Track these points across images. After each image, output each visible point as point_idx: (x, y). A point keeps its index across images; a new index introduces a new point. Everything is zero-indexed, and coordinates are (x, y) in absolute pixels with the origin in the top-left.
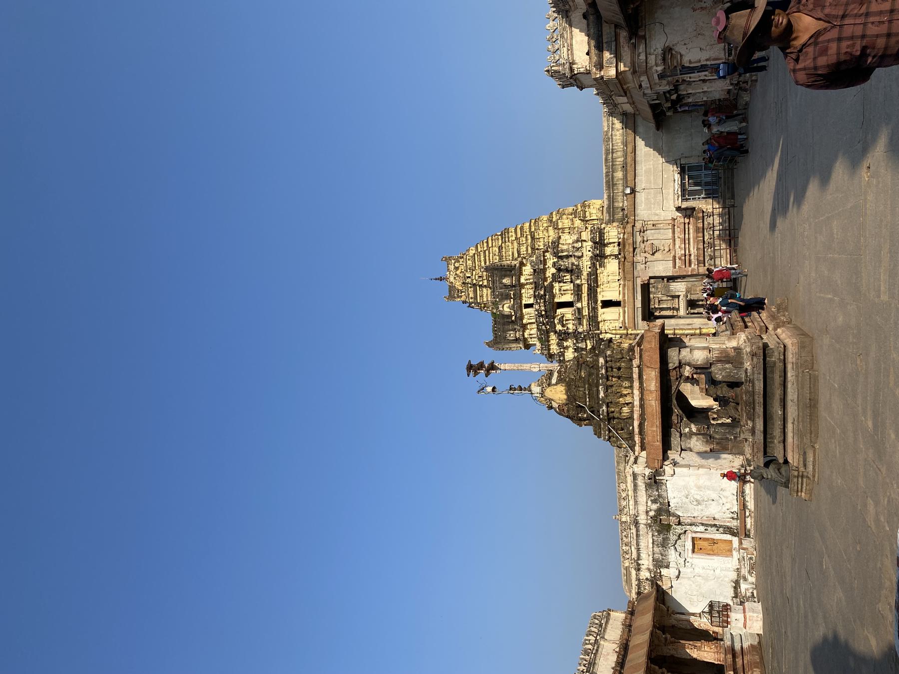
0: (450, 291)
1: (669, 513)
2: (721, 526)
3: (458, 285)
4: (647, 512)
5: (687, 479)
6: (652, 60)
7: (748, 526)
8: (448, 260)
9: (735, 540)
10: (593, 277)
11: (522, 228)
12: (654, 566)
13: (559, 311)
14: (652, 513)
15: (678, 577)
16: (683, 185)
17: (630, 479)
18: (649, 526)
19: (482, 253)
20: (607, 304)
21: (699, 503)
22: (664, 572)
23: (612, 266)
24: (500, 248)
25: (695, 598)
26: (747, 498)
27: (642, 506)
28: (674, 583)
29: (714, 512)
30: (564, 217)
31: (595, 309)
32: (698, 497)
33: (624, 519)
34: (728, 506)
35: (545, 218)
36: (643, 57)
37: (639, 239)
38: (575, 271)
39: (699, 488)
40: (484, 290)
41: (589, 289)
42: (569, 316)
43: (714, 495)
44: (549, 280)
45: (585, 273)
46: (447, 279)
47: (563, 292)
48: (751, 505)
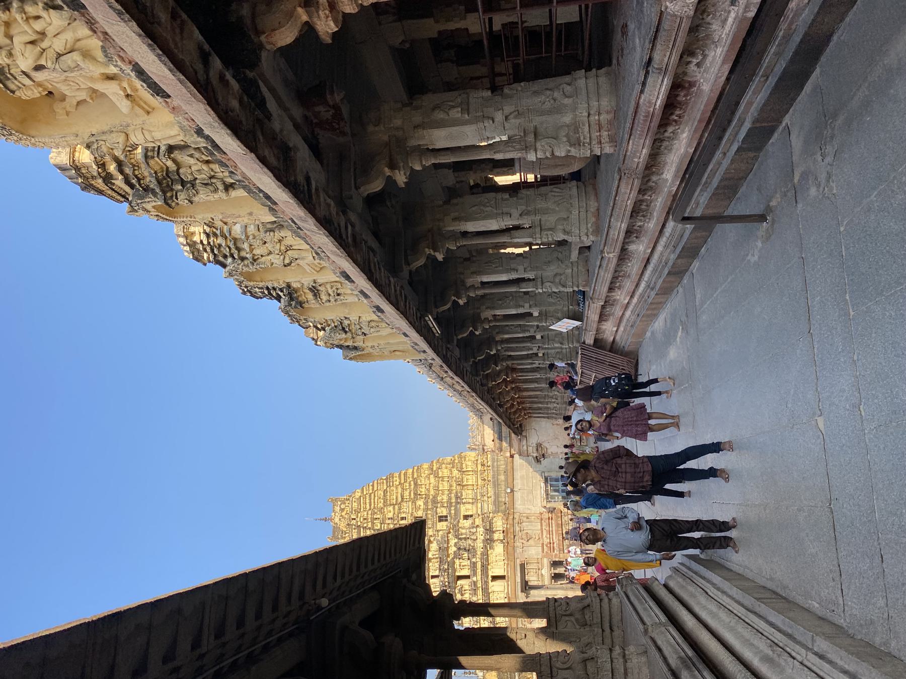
0: (334, 532)
3: (342, 526)
6: (530, 449)
10: (485, 555)
11: (405, 474)
13: (459, 582)
16: (546, 491)
20: (495, 578)
23: (499, 549)
24: (385, 492)
30: (444, 466)
31: (486, 583)
35: (426, 466)
36: (525, 448)
37: (518, 529)
38: (471, 551)
41: (482, 566)
42: (466, 587)
44: (451, 556)
45: (479, 553)
46: (331, 520)
47: (462, 567)
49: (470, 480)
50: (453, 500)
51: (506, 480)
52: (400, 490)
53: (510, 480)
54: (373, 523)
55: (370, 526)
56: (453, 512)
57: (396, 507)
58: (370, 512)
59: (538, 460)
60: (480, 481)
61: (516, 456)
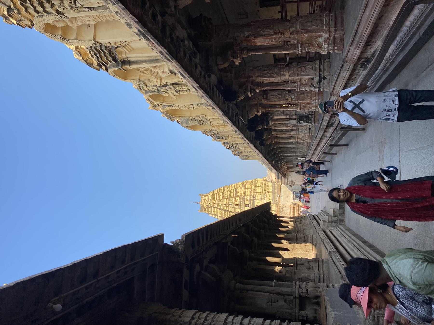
0: (201, 208)
3: (205, 206)
6: (289, 182)
8: (201, 196)
11: (231, 186)
16: (293, 197)
24: (223, 193)
35: (240, 183)
37: (281, 210)
46: (200, 203)
49: (259, 190)
50: (252, 198)
51: (278, 192)
52: (229, 193)
53: (279, 192)
54: (218, 206)
55: (216, 206)
57: (228, 200)
59: (291, 186)
60: (263, 191)
61: (283, 185)
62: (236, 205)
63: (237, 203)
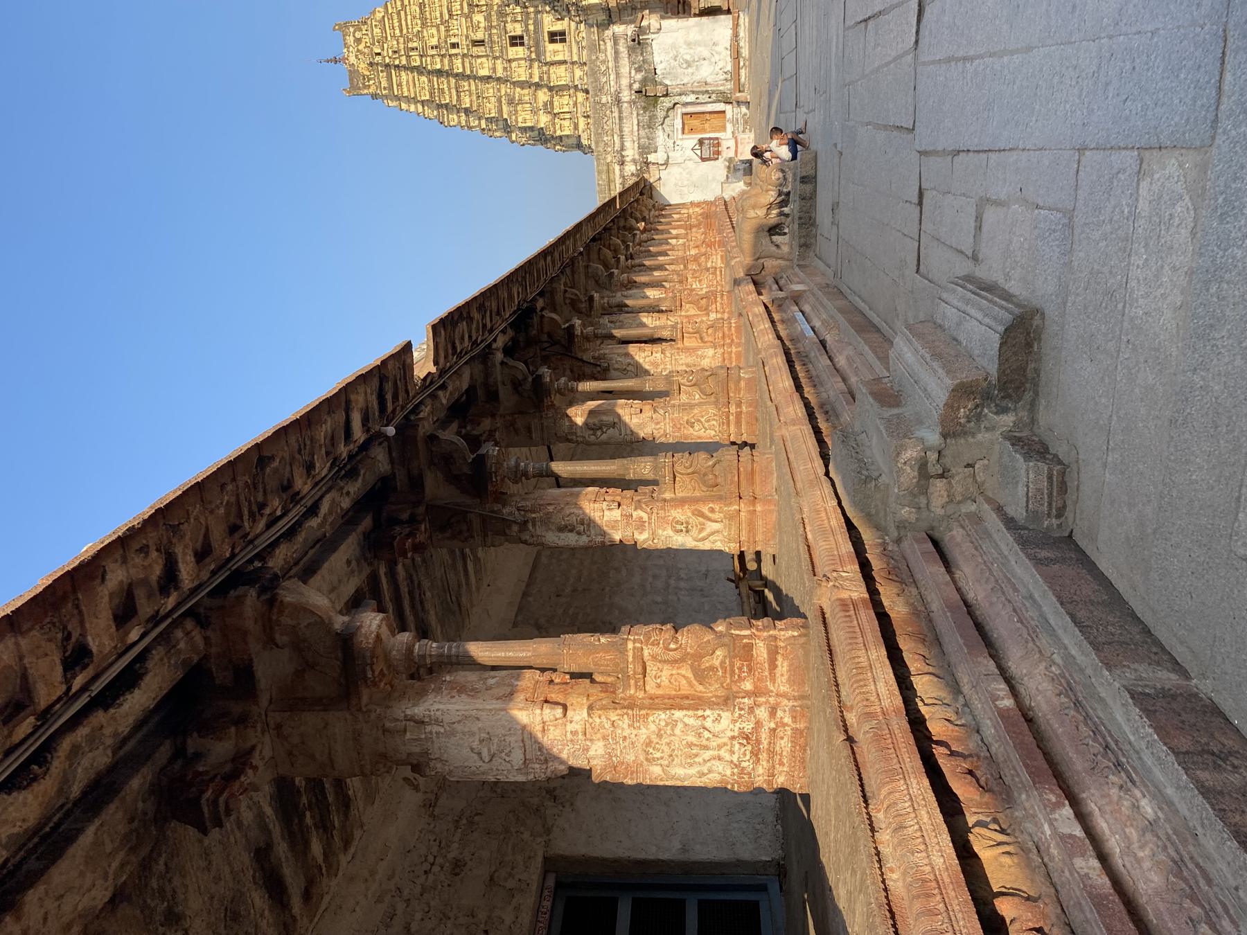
0: (351, 80)
1: (655, 83)
2: (713, 92)
3: (363, 67)
4: (631, 86)
5: (675, 34)
7: (743, 80)
9: (728, 108)
12: (641, 154)
14: (636, 86)
15: (666, 164)
17: (609, 44)
18: (632, 103)
19: (395, 17)
21: (689, 65)
22: (651, 158)
25: (685, 189)
26: (742, 44)
27: (626, 78)
28: (663, 174)
29: (705, 74)
32: (688, 57)
33: (604, 100)
34: (721, 64)
39: (689, 44)
40: (403, 73)
43: (706, 53)
46: (345, 59)
48: (745, 52)
54: (408, 57)
56: (531, 28)
57: (442, 28)
58: (401, 40)
62: (477, 43)
63: (479, 35)
